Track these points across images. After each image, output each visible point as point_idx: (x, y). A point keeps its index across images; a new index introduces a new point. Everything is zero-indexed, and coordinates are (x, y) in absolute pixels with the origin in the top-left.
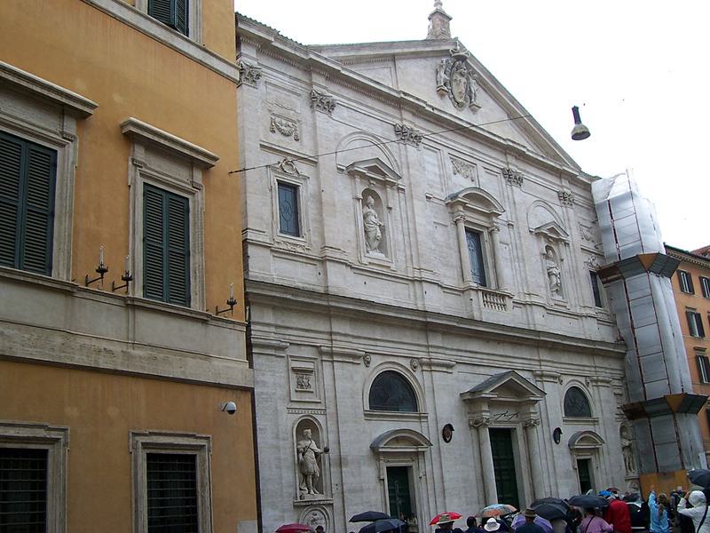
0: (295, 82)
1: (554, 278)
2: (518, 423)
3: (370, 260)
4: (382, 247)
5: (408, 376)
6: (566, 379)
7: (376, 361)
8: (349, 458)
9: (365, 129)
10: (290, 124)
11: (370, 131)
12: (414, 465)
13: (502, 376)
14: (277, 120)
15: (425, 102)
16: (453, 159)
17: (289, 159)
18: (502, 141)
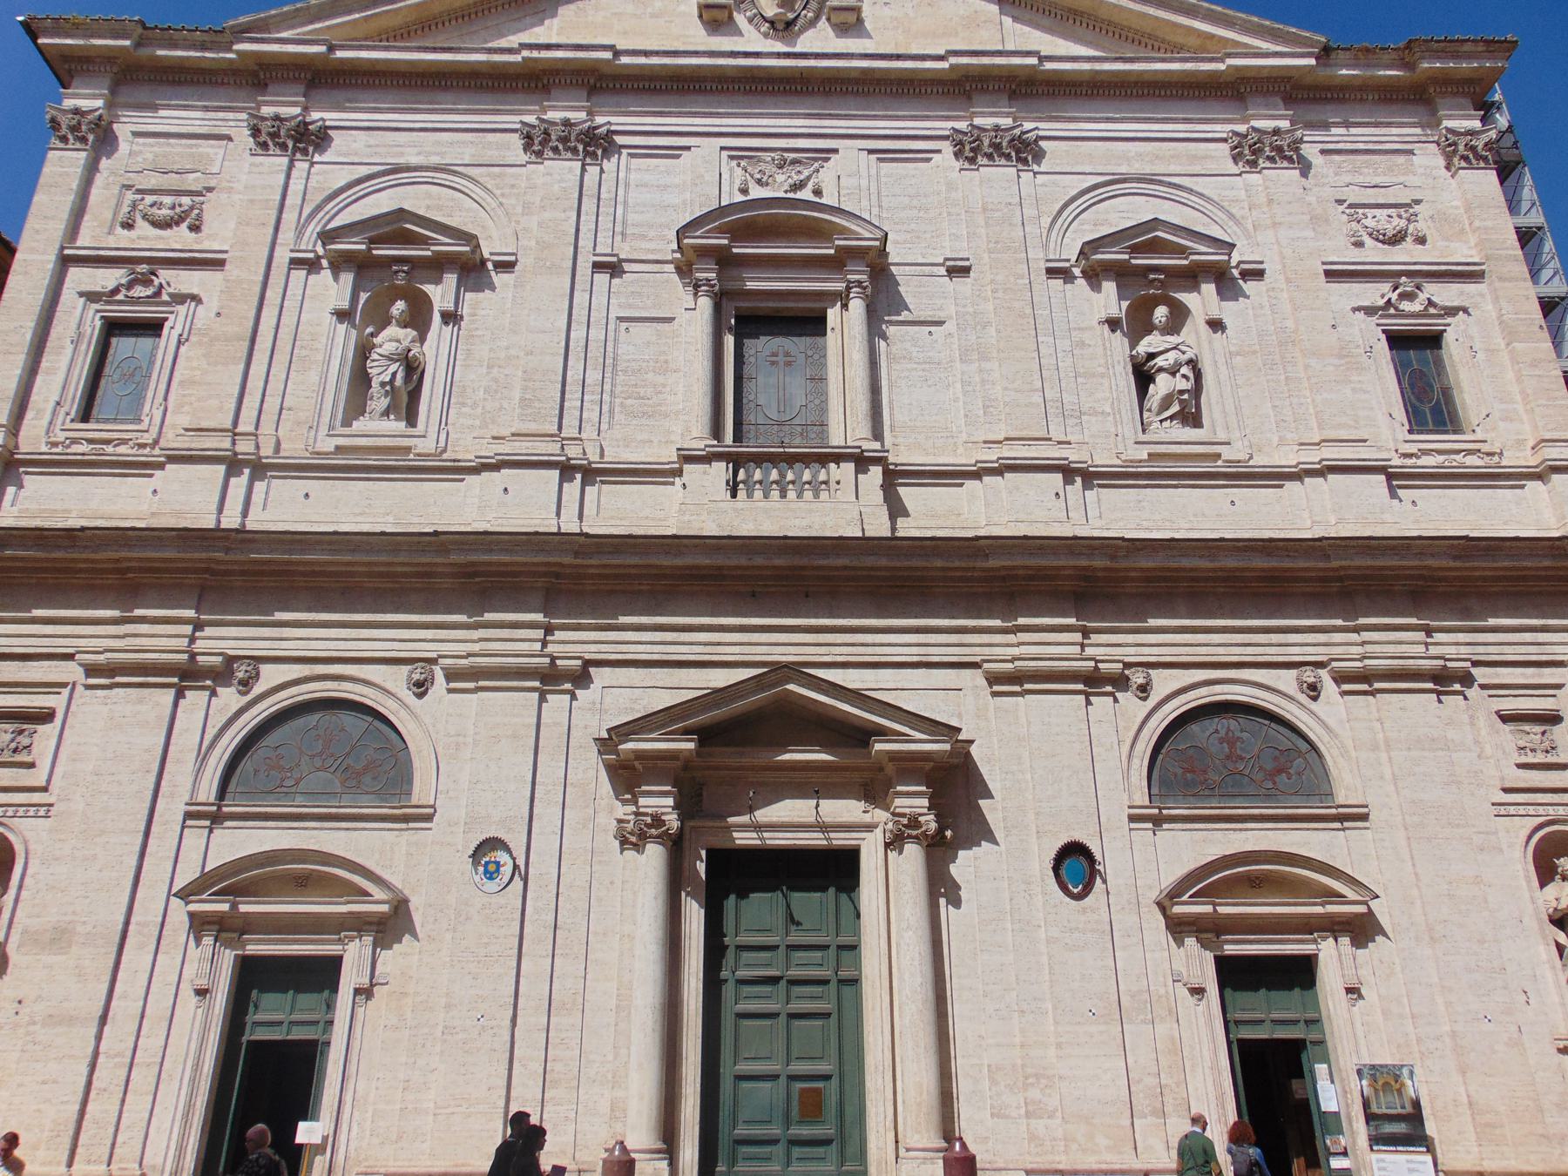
0: (221, 115)
1: (1162, 386)
2: (870, 827)
3: (341, 441)
4: (407, 404)
5: (387, 707)
6: (1165, 681)
7: (271, 675)
8: (80, 929)
9: (414, 160)
10: (186, 201)
11: (435, 160)
12: (355, 954)
13: (756, 683)
14: (149, 199)
15: (611, 48)
16: (737, 155)
17: (143, 268)
18: (928, 65)
